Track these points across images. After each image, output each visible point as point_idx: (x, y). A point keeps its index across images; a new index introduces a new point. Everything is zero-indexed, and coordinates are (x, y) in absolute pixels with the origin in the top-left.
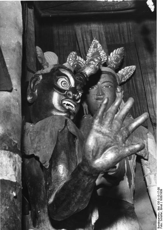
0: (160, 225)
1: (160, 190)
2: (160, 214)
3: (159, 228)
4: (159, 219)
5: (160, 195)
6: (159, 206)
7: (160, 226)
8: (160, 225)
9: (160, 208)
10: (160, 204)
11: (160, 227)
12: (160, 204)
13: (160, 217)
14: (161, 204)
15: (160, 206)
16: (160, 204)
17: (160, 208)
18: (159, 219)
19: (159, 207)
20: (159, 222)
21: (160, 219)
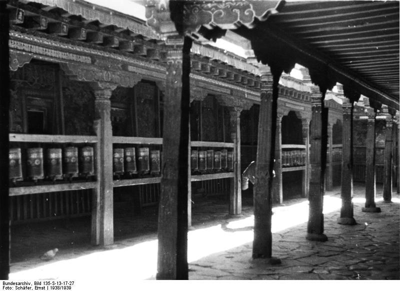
0: (10, 286)
1: (69, 285)
2: (28, 286)
3: (4, 283)
4: (20, 284)
5: (60, 286)
6: (42, 283)
7: (7, 286)
8: (10, 286)
9: (39, 286)
10: (46, 286)
11: (5, 285)
12: (45, 286)
13: (22, 286)
14: (46, 288)
15: (41, 286)
16: (45, 286)
17: (39, 286)
18: (20, 284)
19: (40, 284)
20: (14, 284)
21: (19, 286)
